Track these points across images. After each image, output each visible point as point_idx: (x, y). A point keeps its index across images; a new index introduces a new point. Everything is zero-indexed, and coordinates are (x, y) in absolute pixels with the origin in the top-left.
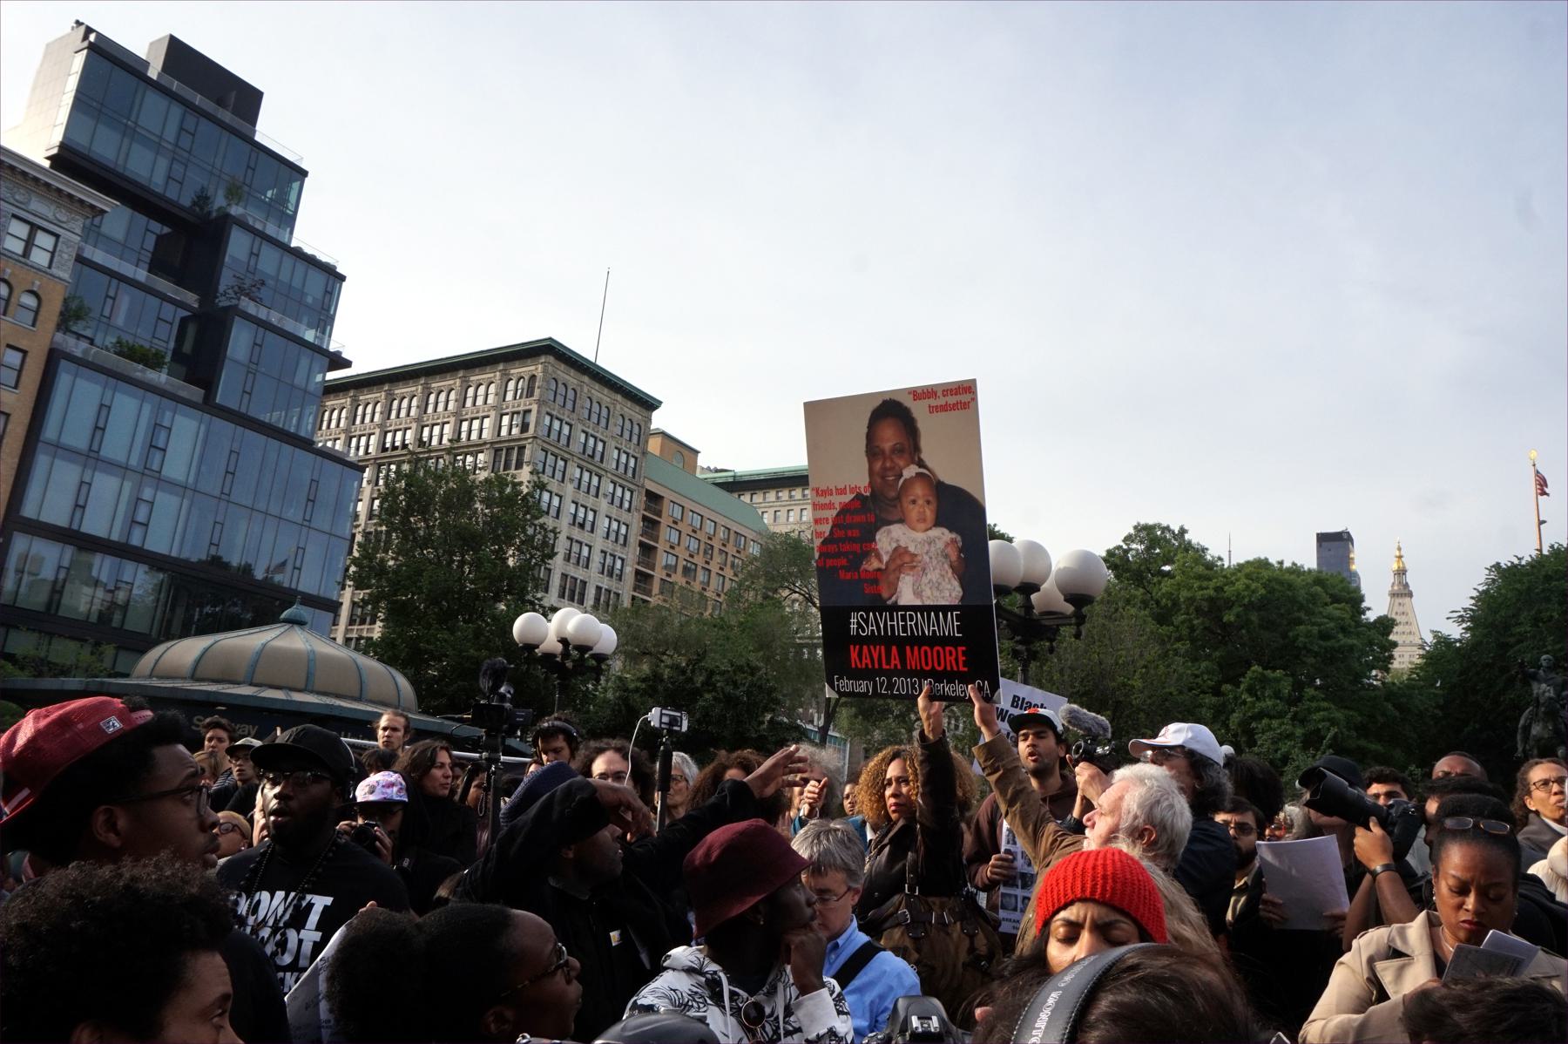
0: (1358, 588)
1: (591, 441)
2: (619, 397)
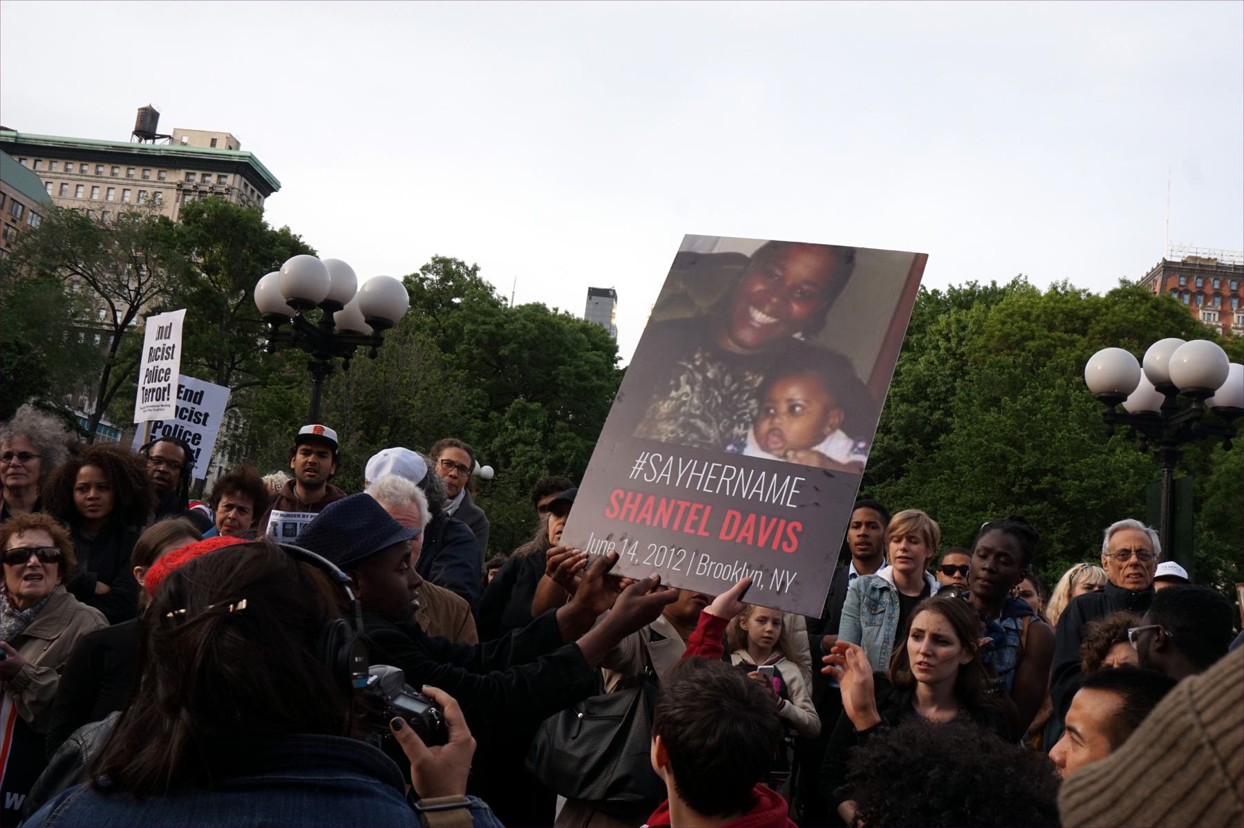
0: (615, 340)
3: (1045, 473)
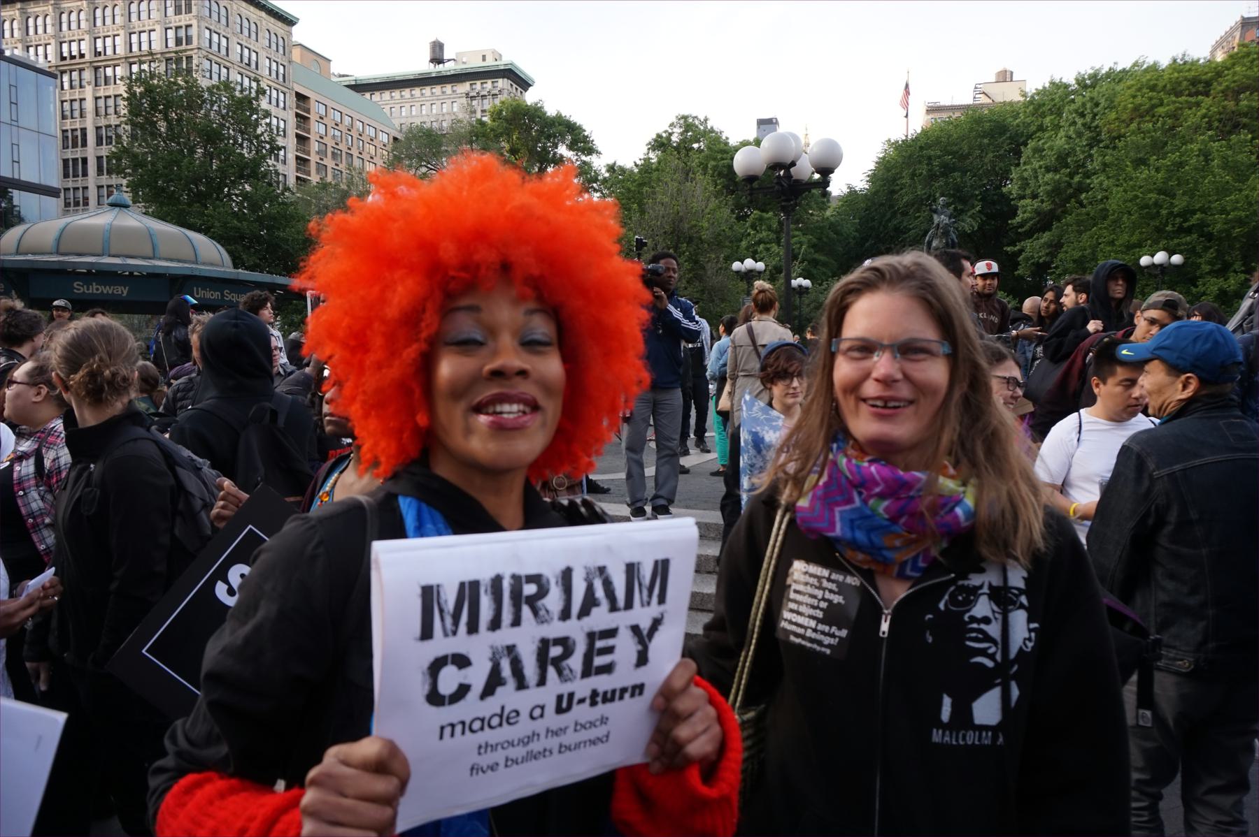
1: (246, 51)
2: (263, 14)
3: (1194, 212)
